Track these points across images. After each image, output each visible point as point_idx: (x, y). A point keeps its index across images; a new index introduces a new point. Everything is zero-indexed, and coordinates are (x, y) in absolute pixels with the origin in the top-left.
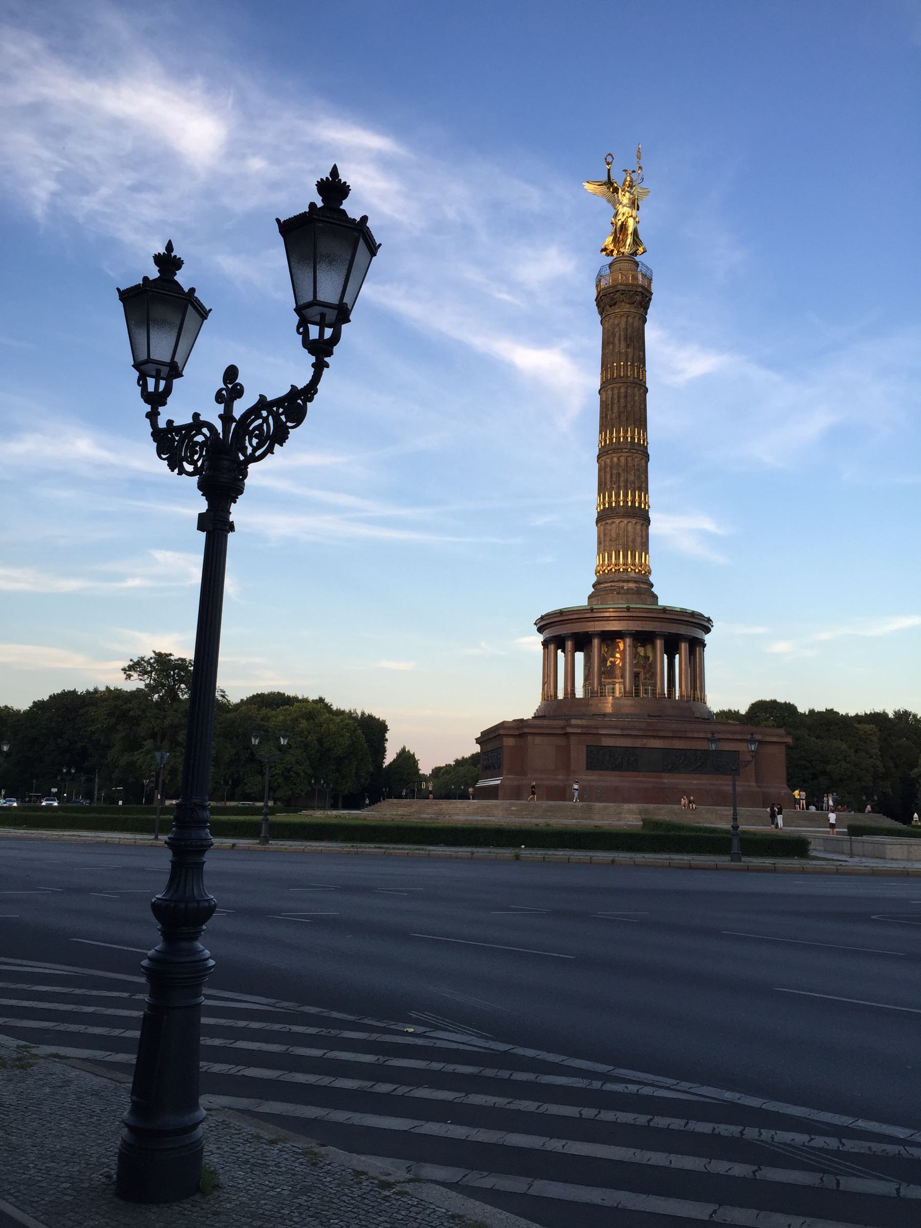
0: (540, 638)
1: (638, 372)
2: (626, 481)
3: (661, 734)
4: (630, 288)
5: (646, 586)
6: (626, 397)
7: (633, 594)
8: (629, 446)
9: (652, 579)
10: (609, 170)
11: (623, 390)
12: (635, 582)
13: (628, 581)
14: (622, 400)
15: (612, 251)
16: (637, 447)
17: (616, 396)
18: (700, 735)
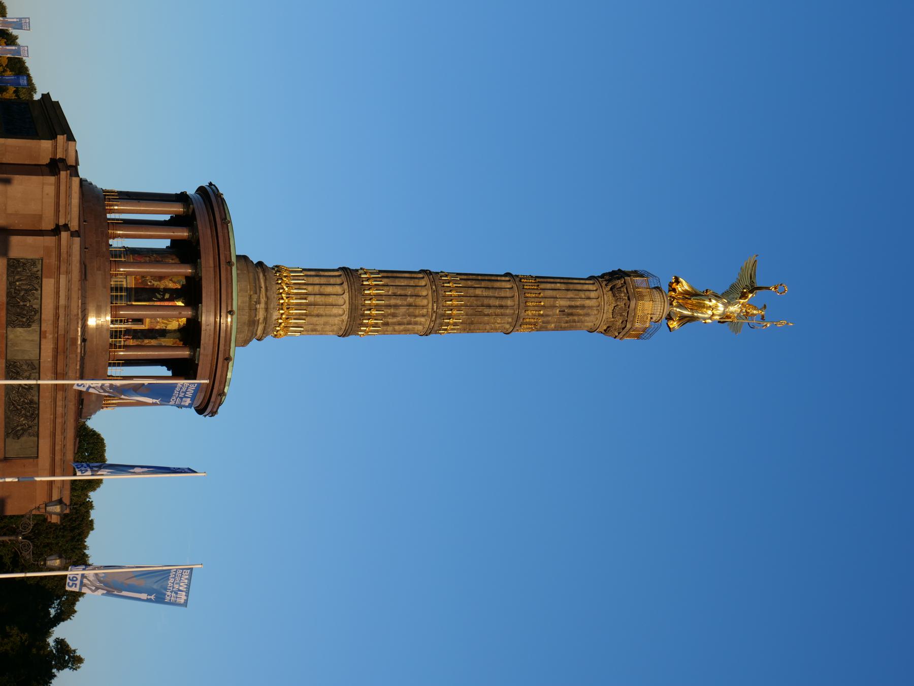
0: (191, 191)
1: (530, 324)
2: (396, 306)
3: (60, 358)
4: (632, 314)
5: (259, 332)
6: (501, 307)
7: (250, 316)
8: (440, 311)
9: (269, 339)
10: (768, 288)
11: (509, 303)
12: (265, 319)
13: (267, 309)
14: (497, 303)
15: (674, 290)
16: (438, 321)
18: (60, 410)
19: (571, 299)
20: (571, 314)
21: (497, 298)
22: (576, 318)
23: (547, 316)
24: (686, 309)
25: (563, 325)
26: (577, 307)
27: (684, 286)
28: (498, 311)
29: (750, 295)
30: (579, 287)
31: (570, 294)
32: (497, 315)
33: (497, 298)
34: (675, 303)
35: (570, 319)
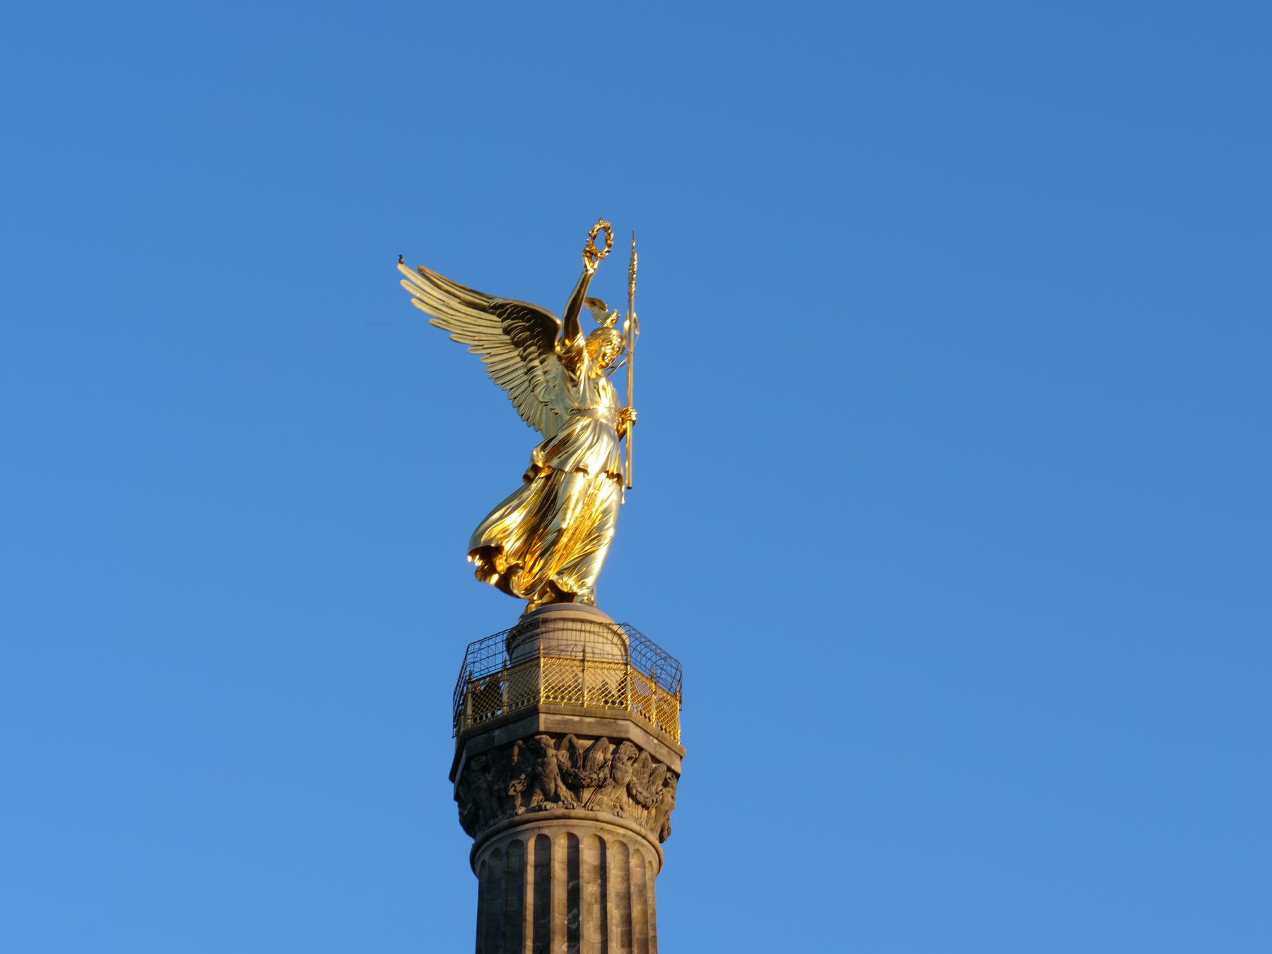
29: (580, 341)
30: (559, 893)
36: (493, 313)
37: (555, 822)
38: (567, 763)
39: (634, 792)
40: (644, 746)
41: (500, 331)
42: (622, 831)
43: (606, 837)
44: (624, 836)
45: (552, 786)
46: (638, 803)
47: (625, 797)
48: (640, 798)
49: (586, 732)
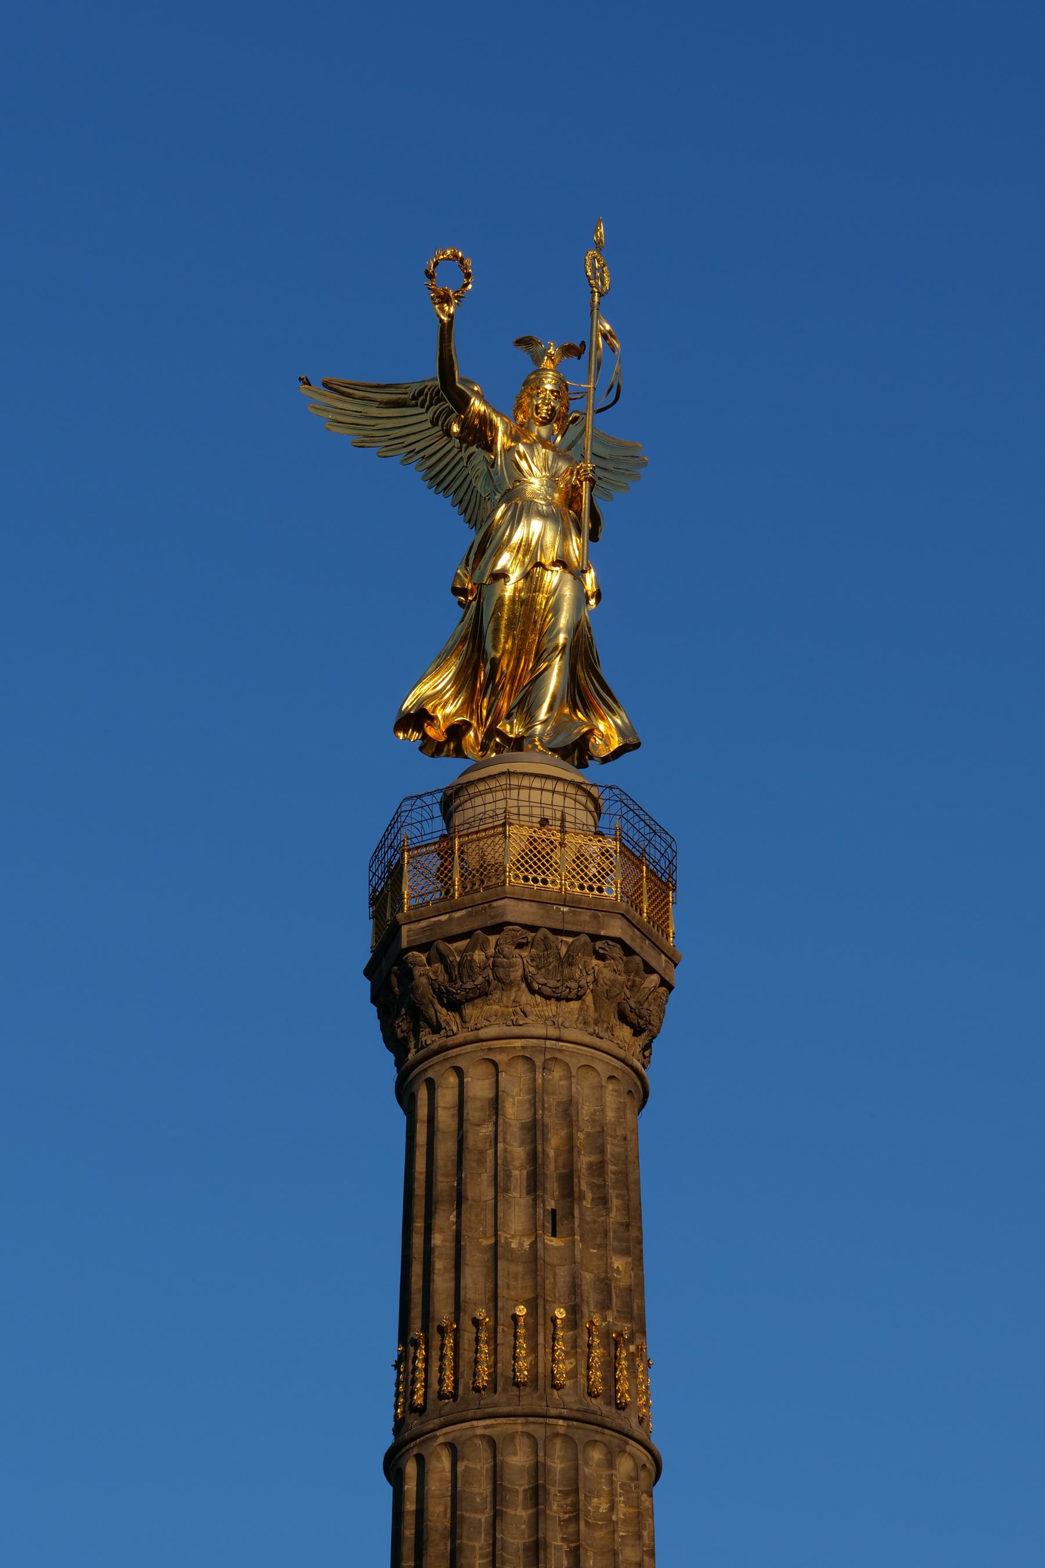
1: (611, 1365)
10: (446, 331)
14: (519, 1513)
15: (457, 732)
17: (482, 1489)
19: (499, 1185)
20: (568, 1180)
21: (497, 1515)
22: (584, 1160)
23: (575, 1287)
24: (538, 678)
25: (615, 1216)
26: (534, 1159)
27: (437, 690)
28: (556, 1507)
29: (477, 405)
30: (445, 1149)
31: (479, 1188)
32: (575, 1514)
33: (497, 1515)
34: (514, 729)
35: (588, 1189)
36: (416, 405)
37: (436, 1059)
38: (443, 977)
39: (536, 986)
40: (538, 923)
41: (428, 425)
42: (518, 1043)
43: (497, 1057)
44: (523, 1048)
45: (432, 1012)
46: (548, 998)
47: (525, 997)
48: (547, 991)
49: (457, 930)
